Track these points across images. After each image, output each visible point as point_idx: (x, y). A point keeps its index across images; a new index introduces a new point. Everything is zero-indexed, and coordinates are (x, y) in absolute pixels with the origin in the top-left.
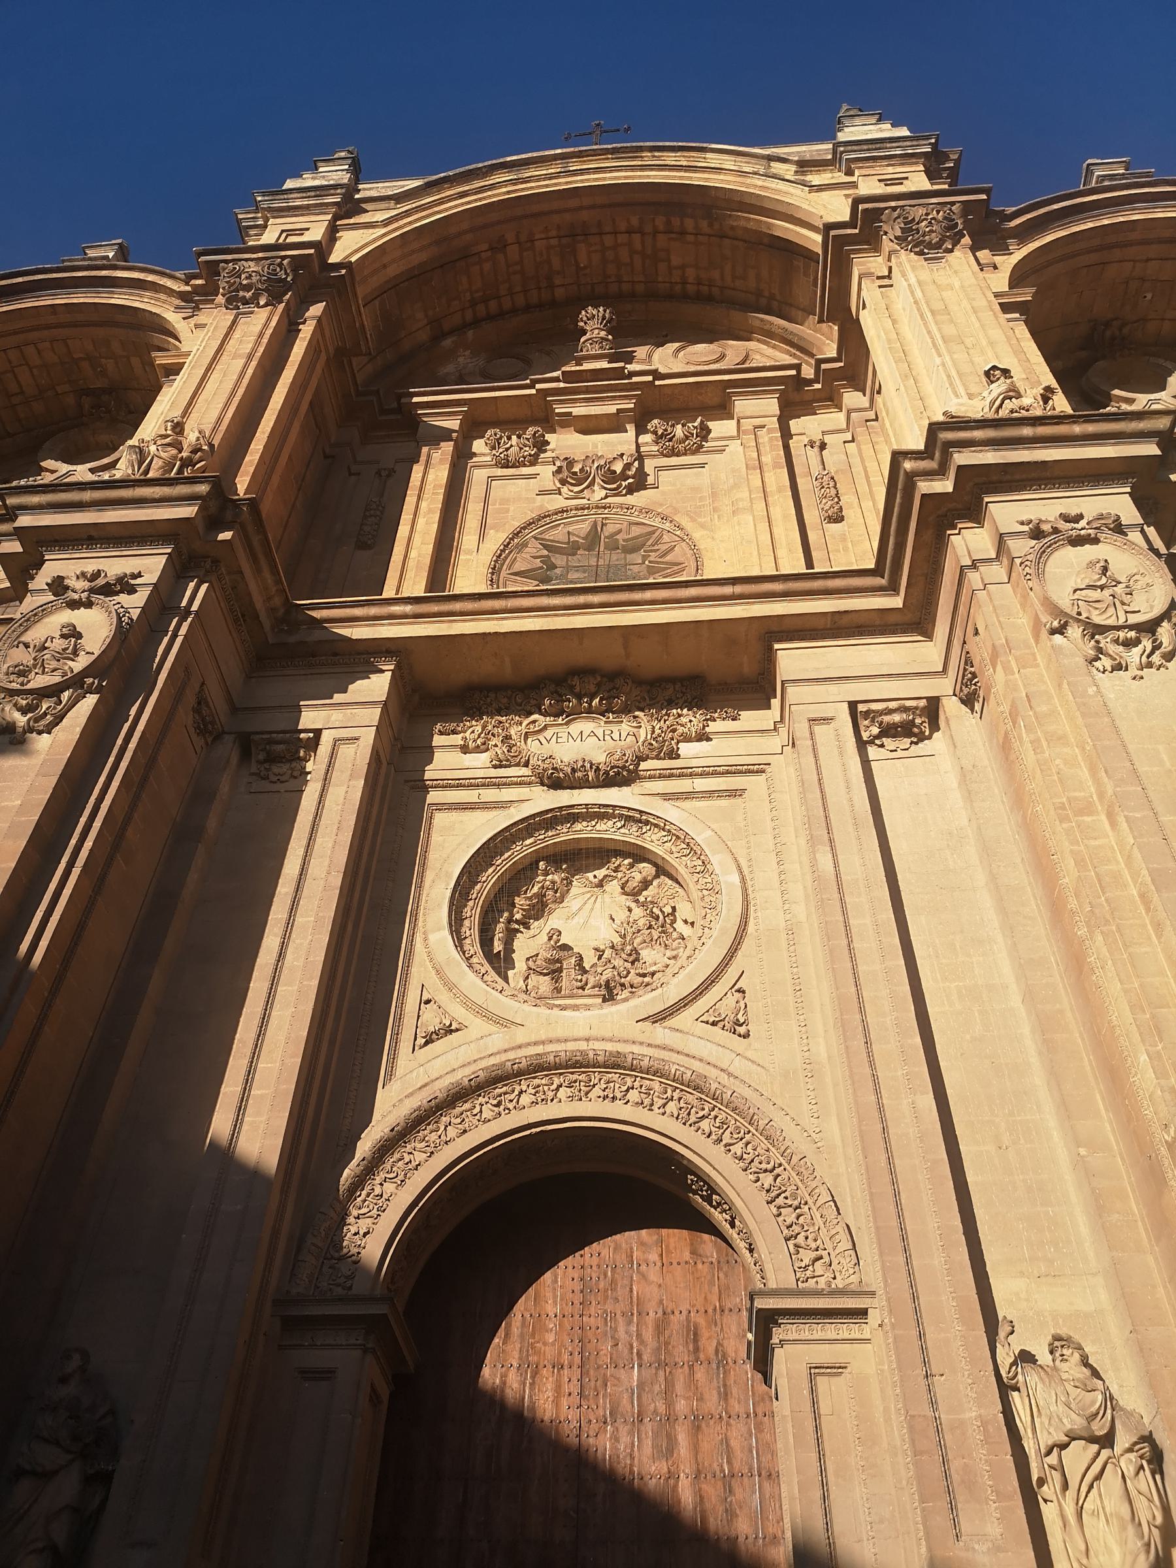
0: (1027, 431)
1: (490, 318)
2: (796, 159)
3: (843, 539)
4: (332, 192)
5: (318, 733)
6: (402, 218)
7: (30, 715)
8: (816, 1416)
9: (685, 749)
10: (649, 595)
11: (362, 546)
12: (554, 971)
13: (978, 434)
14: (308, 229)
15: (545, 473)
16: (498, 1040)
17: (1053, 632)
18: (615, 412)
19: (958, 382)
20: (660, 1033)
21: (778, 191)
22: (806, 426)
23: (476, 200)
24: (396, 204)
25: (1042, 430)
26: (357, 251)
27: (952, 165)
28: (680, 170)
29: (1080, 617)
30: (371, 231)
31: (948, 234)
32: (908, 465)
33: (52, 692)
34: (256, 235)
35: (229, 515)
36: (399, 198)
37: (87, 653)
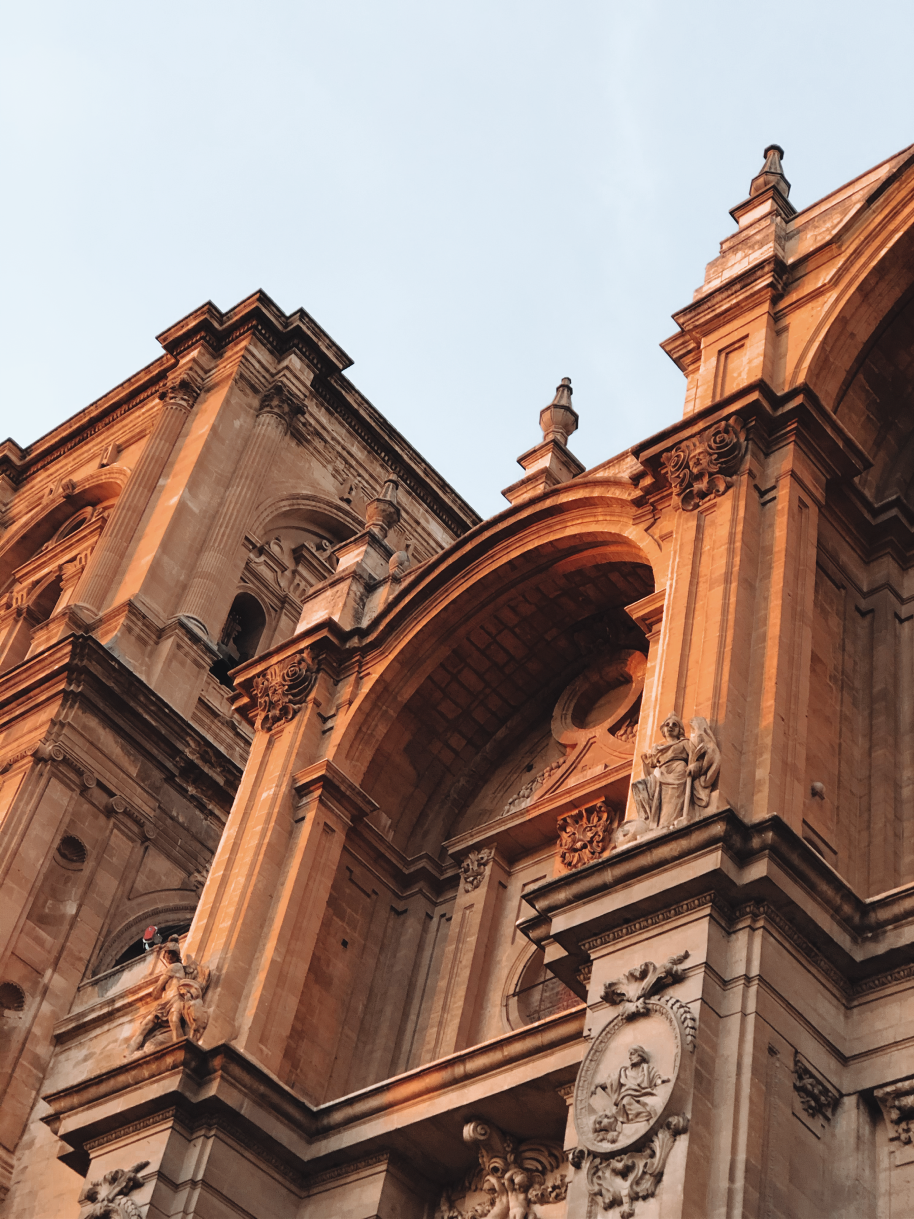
4: (759, 273)
6: (852, 263)
7: (631, 1177)
14: (747, 336)
24: (840, 247)
30: (821, 300)
33: (642, 1145)
34: (693, 362)
35: (756, 842)
37: (663, 1082)
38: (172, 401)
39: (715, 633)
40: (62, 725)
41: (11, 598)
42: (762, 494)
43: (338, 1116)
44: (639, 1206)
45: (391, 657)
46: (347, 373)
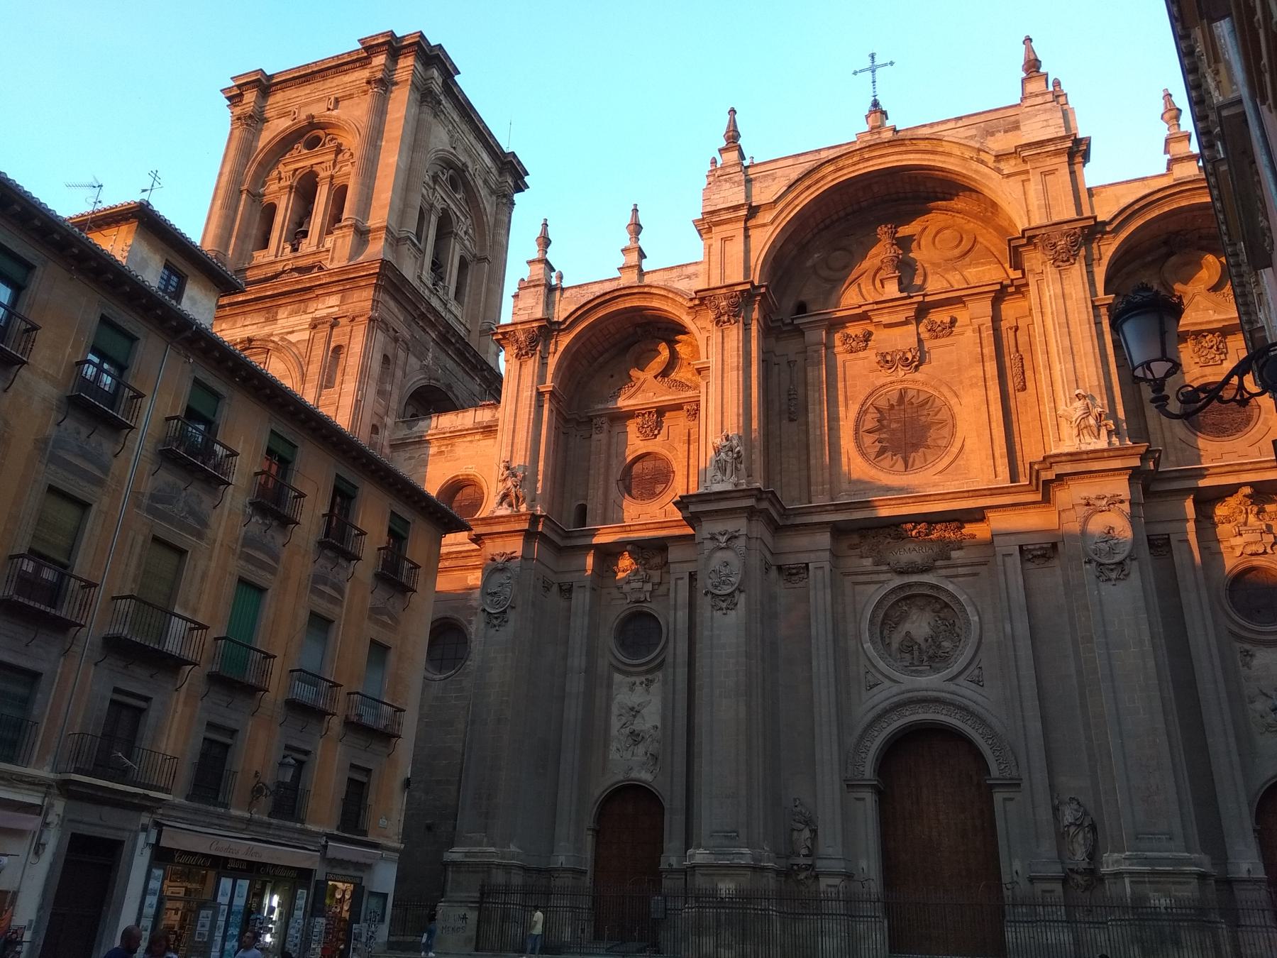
0: (1085, 457)
1: (827, 227)
2: (994, 153)
3: (1026, 404)
5: (807, 564)
8: (1005, 811)
9: (954, 554)
10: (932, 498)
11: (791, 420)
12: (911, 652)
13: (1064, 458)
15: (870, 356)
16: (895, 689)
17: (1085, 562)
18: (904, 319)
19: (1066, 386)
20: (952, 687)
21: (984, 175)
22: (1010, 310)
23: (815, 191)
25: (1091, 456)
26: (762, 250)
27: (1085, 148)
28: (928, 153)
29: (1096, 558)
31: (1072, 253)
32: (1036, 467)
33: (731, 594)
35: (764, 496)
36: (775, 202)
38: (376, 90)
39: (735, 391)
40: (378, 302)
41: (280, 173)
42: (745, 324)
43: (576, 534)
44: (729, 611)
45: (572, 336)
46: (457, 78)
